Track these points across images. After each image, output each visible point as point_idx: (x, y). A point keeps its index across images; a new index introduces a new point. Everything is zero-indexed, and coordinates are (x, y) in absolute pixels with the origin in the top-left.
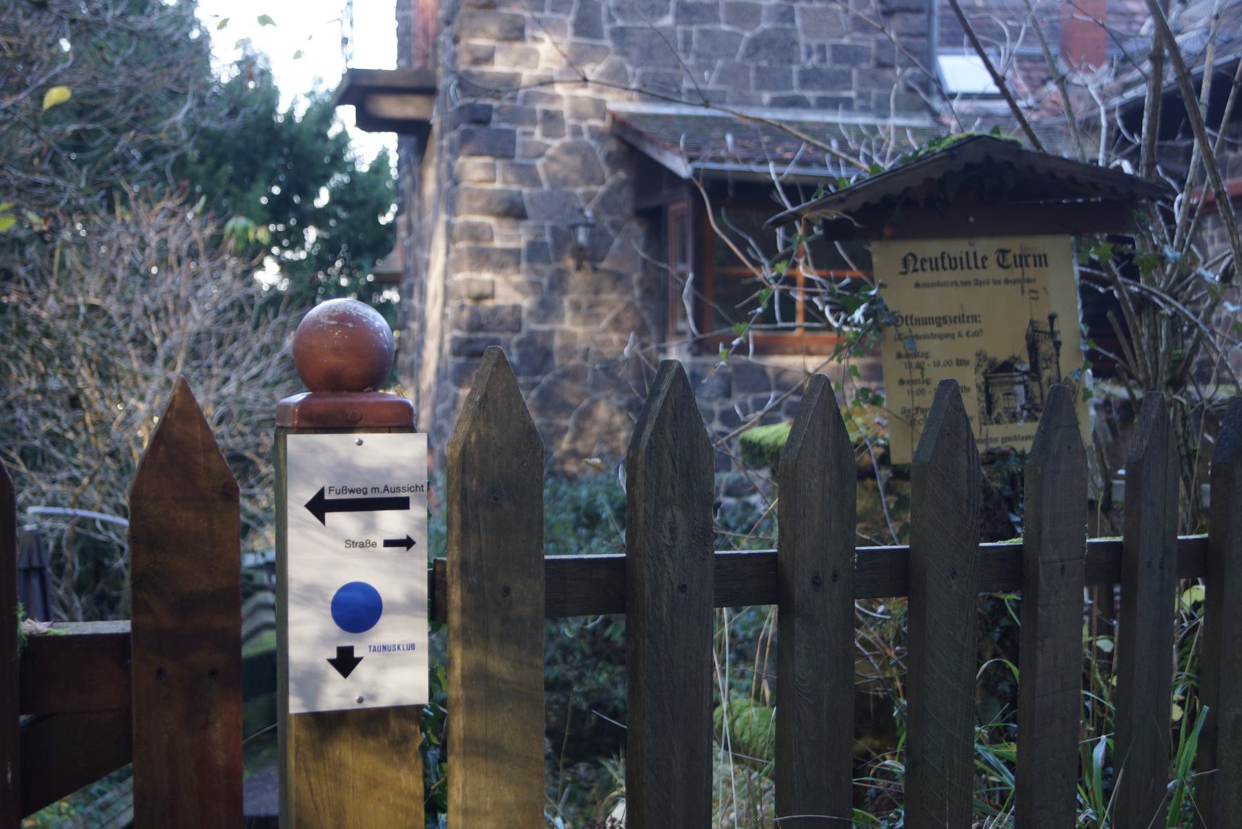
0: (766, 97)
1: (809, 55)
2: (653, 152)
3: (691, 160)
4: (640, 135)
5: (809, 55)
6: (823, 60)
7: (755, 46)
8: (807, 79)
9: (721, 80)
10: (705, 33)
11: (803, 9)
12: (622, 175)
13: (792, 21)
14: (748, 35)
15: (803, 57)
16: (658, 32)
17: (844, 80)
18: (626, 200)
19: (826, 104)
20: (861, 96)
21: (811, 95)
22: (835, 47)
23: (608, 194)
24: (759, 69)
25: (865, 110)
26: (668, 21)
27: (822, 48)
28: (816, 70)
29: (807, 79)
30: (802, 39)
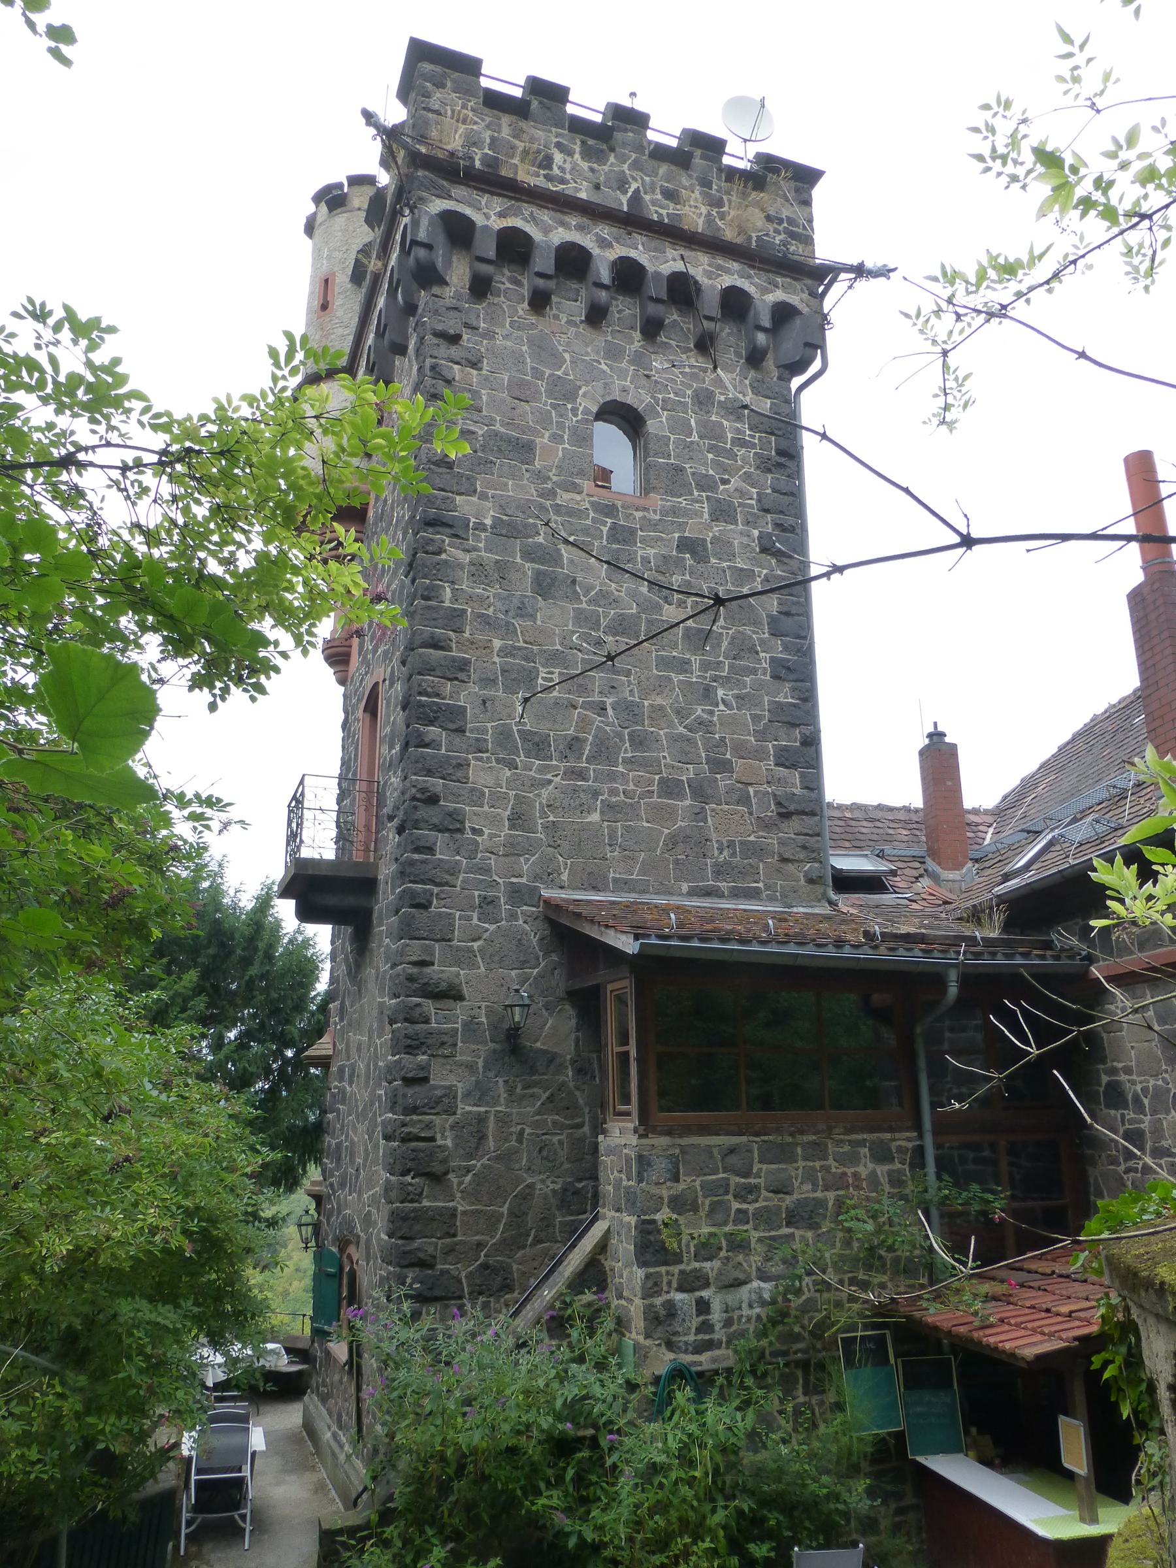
0: (685, 887)
1: (721, 850)
2: (593, 932)
3: (637, 937)
4: (578, 915)
5: (721, 850)
6: (733, 855)
7: (673, 842)
8: (720, 871)
9: (642, 871)
10: (627, 829)
11: (713, 810)
12: (554, 957)
13: (705, 820)
14: (666, 831)
15: (716, 852)
16: (586, 827)
17: (753, 872)
18: (559, 983)
19: (736, 894)
20: (767, 887)
21: (723, 885)
22: (741, 843)
23: (541, 976)
24: (677, 862)
25: (772, 899)
26: (595, 817)
27: (731, 844)
28: (726, 863)
29: (720, 871)
30: (714, 836)
